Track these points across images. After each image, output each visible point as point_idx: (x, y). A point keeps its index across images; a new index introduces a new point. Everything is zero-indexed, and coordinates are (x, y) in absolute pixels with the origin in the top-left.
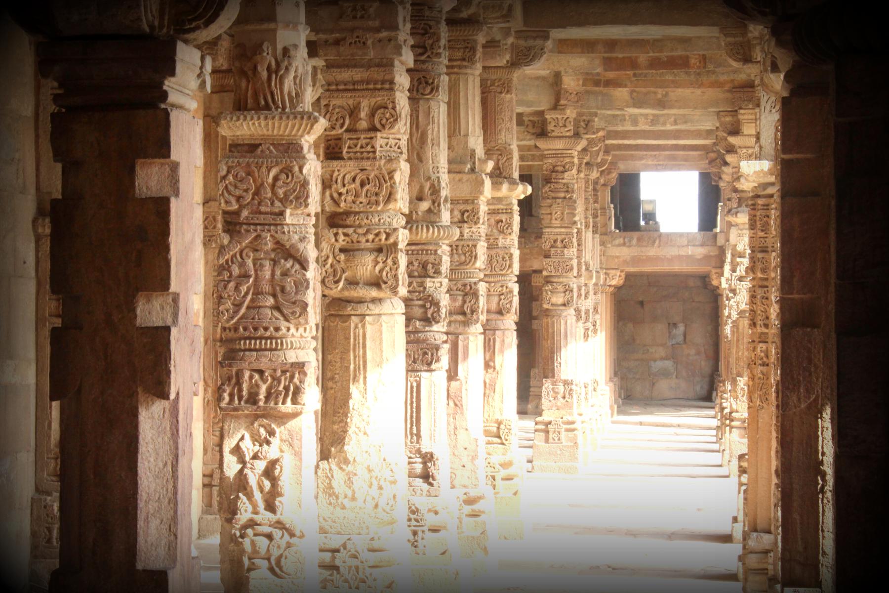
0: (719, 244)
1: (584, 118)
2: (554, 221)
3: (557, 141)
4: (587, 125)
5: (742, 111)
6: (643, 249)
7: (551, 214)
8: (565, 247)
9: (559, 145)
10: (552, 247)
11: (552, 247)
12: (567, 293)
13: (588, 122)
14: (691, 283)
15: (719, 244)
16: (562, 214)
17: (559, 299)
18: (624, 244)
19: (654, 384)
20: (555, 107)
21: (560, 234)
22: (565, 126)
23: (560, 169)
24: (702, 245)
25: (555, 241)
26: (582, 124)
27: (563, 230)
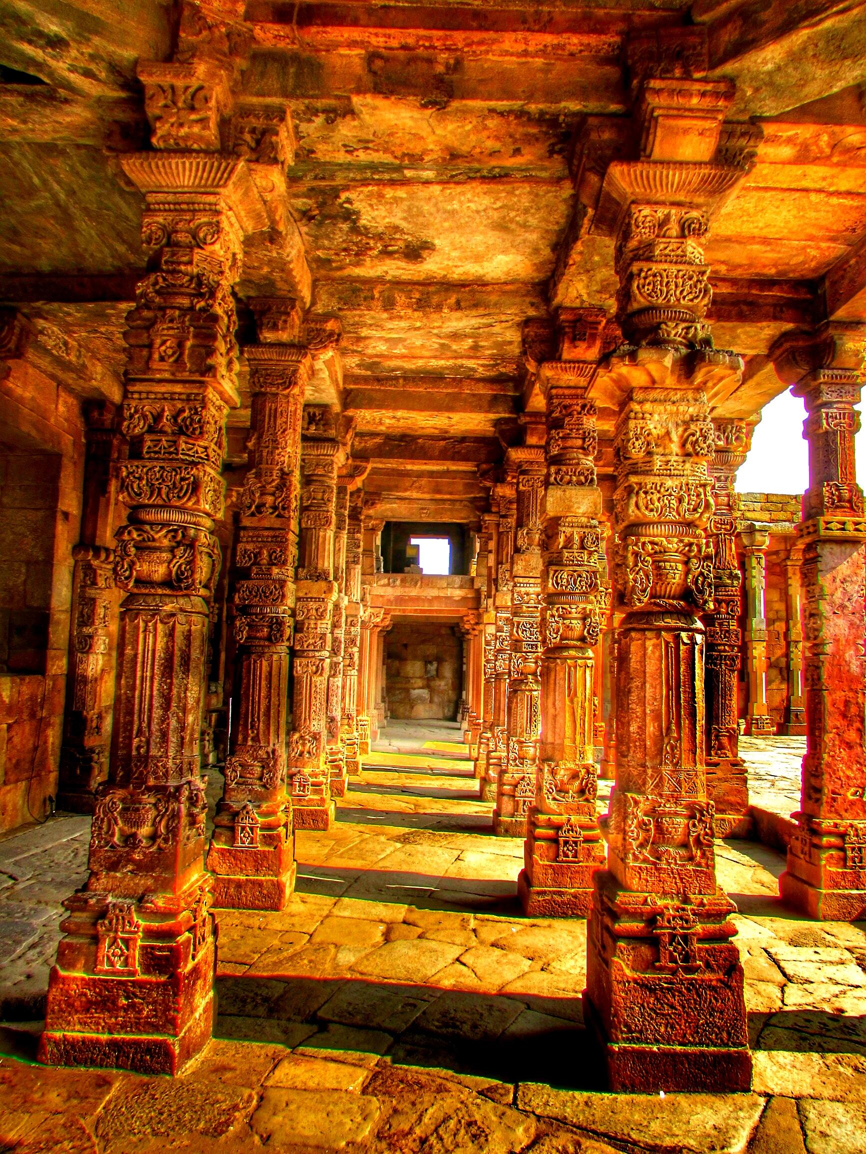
0: (476, 587)
1: (254, 122)
2: (155, 365)
3: (175, 161)
4: (258, 142)
5: (655, 84)
6: (407, 590)
7: (150, 346)
8: (181, 432)
9: (183, 174)
11: (151, 430)
12: (179, 551)
13: (264, 133)
14: (443, 631)
15: (476, 587)
16: (181, 345)
18: (389, 585)
19: (412, 708)
20: (172, 54)
21: (172, 397)
22: (192, 109)
24: (461, 587)
25: (158, 418)
26: (247, 137)
27: (178, 388)
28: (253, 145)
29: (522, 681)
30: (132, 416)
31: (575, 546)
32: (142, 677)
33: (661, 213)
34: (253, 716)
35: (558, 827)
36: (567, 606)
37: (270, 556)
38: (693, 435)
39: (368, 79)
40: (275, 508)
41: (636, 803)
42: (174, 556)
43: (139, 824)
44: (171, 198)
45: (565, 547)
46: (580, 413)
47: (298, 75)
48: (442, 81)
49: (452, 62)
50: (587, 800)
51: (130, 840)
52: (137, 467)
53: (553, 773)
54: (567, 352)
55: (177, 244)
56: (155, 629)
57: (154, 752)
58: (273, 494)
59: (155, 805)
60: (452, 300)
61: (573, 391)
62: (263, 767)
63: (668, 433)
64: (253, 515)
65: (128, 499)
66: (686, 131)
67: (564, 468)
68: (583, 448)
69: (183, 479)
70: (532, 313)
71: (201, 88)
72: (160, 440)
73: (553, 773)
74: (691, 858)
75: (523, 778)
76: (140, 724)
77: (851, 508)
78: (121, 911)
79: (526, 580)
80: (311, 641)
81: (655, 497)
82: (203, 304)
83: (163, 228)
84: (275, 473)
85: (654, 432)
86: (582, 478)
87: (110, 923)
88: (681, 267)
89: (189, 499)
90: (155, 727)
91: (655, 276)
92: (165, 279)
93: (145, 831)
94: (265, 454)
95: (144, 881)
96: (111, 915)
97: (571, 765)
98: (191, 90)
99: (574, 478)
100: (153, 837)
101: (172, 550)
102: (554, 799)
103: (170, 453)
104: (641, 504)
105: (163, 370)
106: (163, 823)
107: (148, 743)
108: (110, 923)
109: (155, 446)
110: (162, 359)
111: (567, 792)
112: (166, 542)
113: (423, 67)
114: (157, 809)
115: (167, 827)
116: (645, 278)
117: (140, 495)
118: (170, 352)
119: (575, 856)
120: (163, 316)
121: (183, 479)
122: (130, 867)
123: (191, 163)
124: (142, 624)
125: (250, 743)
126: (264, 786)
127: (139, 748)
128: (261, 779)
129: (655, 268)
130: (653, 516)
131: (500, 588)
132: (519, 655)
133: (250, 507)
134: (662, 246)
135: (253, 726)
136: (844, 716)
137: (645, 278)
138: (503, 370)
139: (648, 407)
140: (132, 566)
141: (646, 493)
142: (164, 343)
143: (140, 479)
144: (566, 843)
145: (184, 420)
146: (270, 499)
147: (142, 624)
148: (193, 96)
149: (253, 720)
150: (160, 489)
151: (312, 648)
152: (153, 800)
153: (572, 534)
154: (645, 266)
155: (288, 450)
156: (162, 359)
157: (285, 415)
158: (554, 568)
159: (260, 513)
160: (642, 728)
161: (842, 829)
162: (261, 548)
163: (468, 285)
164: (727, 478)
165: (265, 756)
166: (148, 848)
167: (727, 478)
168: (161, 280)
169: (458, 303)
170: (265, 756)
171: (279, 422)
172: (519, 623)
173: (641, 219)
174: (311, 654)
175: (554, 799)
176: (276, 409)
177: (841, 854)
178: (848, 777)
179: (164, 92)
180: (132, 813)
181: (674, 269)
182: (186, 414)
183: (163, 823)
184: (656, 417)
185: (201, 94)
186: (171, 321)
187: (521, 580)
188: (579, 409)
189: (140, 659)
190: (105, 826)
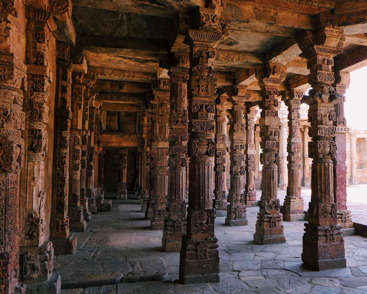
4: (223, 28)
7: (199, 86)
8: (208, 112)
10: (199, 111)
11: (199, 111)
12: (210, 145)
16: (207, 87)
17: (204, 149)
23: (205, 55)
25: (202, 106)
27: (207, 99)
28: (222, 29)
29: (236, 175)
30: (194, 107)
31: (273, 135)
32: (202, 180)
33: (324, 57)
34: (178, 190)
35: (270, 218)
36: (271, 153)
37: (181, 138)
38: (331, 115)
39: (254, 15)
40: (182, 122)
41: (321, 204)
42: (209, 147)
43: (203, 220)
44: (201, 43)
45: (270, 135)
46: (273, 94)
47: (235, 11)
48: (273, 17)
49: (275, 12)
50: (277, 210)
51: (201, 224)
52: (197, 121)
53: (268, 202)
54: (271, 76)
55: (202, 57)
56: (205, 167)
57: (206, 200)
58: (182, 117)
59: (207, 214)
60: (237, 57)
61: (272, 87)
62: (181, 206)
63: (326, 115)
64: (175, 124)
65: (195, 130)
66: (332, 41)
67: (269, 111)
68: (274, 104)
69: (209, 125)
70: (260, 62)
71: (216, 16)
72: (203, 114)
73: (268, 202)
74: (332, 217)
75: (238, 207)
76: (202, 193)
77: (343, 124)
78: (203, 243)
79: (237, 141)
80: (164, 163)
81: (324, 130)
82: (211, 75)
83: (198, 51)
84: (182, 110)
85: (323, 114)
86: (274, 114)
87: (200, 246)
88: (328, 72)
89: (212, 131)
90: (206, 194)
91: (322, 74)
92: (200, 67)
93: (205, 222)
94: (178, 104)
95: (206, 235)
96: (200, 244)
97: (273, 200)
98: (213, 16)
99: (272, 114)
100: (207, 223)
101: (208, 145)
102: (268, 210)
103: (206, 118)
104: (321, 132)
105: (203, 93)
106: (210, 219)
107: (205, 198)
108: (200, 246)
109: (202, 116)
110: (202, 91)
111: (272, 208)
112: (206, 143)
113: (268, 13)
114: (208, 215)
115: (211, 220)
116: (320, 75)
117: (198, 129)
118: (204, 89)
119: (275, 226)
120: (202, 78)
121: (209, 125)
122: (202, 231)
123: (209, 35)
124: (201, 166)
125: (177, 199)
126: (182, 212)
127: (202, 199)
128: (181, 210)
129: (323, 72)
130: (323, 135)
131: (217, 142)
132: (236, 166)
133: (174, 122)
134: (324, 67)
135: (178, 194)
136: (341, 182)
137: (320, 75)
138: (231, 70)
139: (321, 108)
140: (197, 149)
141: (321, 129)
142: (203, 86)
143: (198, 125)
144: (272, 222)
145: (209, 108)
146: (180, 119)
147: (201, 166)
148: (214, 17)
149: (178, 192)
150: (204, 128)
151: (165, 166)
152: (206, 213)
153: (272, 131)
154: (320, 71)
155: (185, 103)
156: (202, 91)
157: (184, 91)
158: (267, 141)
159: (178, 124)
160: (321, 187)
161: (341, 213)
162: (178, 135)
163: (242, 53)
164: (297, 108)
165: (182, 203)
166: (206, 226)
167: (297, 108)
168: (199, 67)
169: (239, 58)
170: (182, 203)
171: (182, 93)
172: (235, 155)
173: (319, 59)
174: (164, 168)
175: (268, 210)
176: (181, 89)
177: (341, 219)
178: (342, 199)
179: (206, 16)
180: (201, 218)
181: (326, 72)
182: (210, 107)
183: (210, 219)
184: (323, 110)
185: (215, 18)
186: (204, 80)
187: (236, 141)
188: (273, 93)
189: (201, 176)
190: (194, 221)
